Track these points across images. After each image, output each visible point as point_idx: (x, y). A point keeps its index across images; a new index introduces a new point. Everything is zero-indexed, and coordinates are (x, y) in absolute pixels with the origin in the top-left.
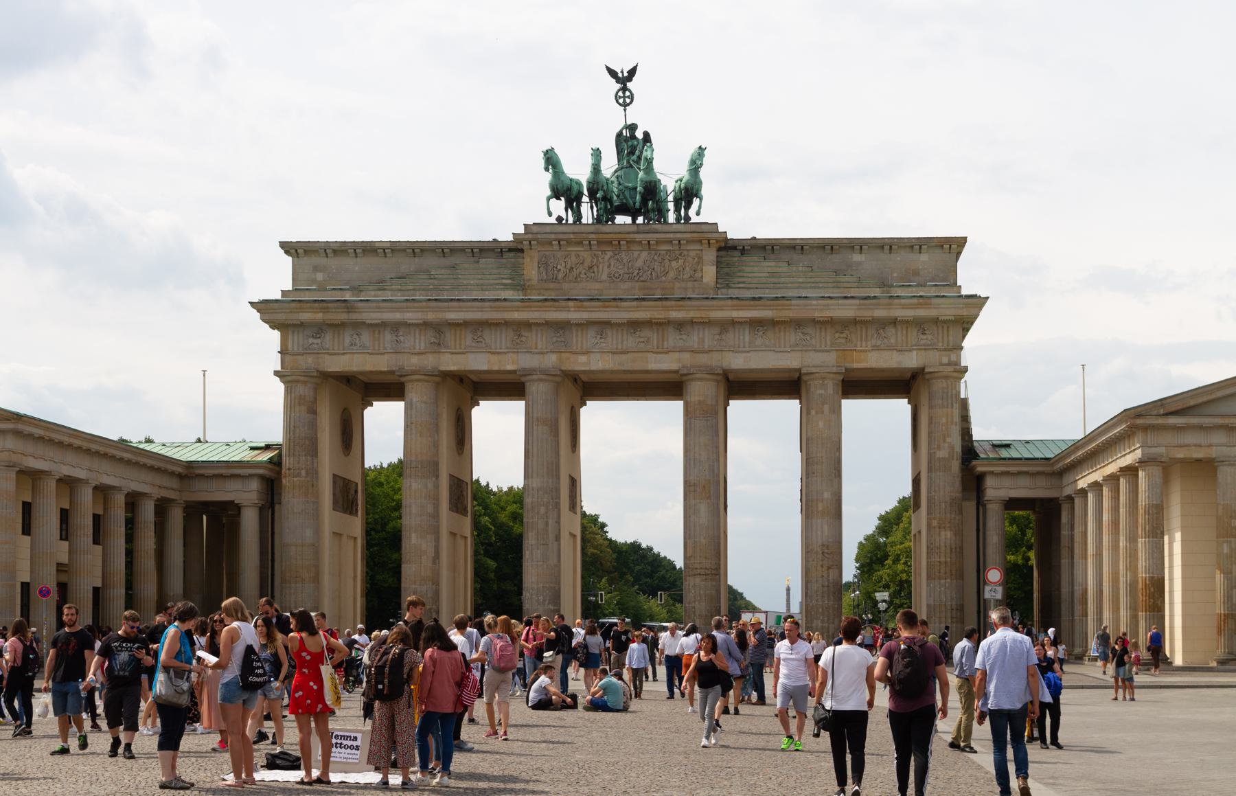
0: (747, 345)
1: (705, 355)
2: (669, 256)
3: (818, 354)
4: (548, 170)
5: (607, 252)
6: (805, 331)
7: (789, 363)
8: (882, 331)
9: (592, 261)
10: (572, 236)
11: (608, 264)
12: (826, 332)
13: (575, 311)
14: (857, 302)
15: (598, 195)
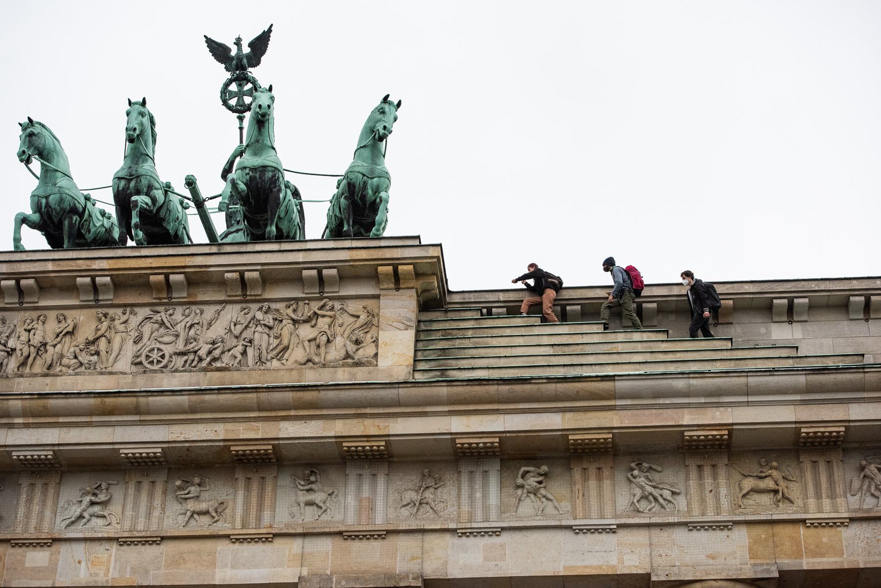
0: (493, 515)
1: (376, 544)
2: (295, 311)
3: (695, 534)
4: (28, 162)
5: (136, 309)
6: (656, 476)
7: (614, 561)
8: (873, 467)
9: (97, 330)
10: (50, 266)
11: (136, 334)
12: (715, 477)
13: (27, 426)
14: (801, 379)
15: (134, 198)
